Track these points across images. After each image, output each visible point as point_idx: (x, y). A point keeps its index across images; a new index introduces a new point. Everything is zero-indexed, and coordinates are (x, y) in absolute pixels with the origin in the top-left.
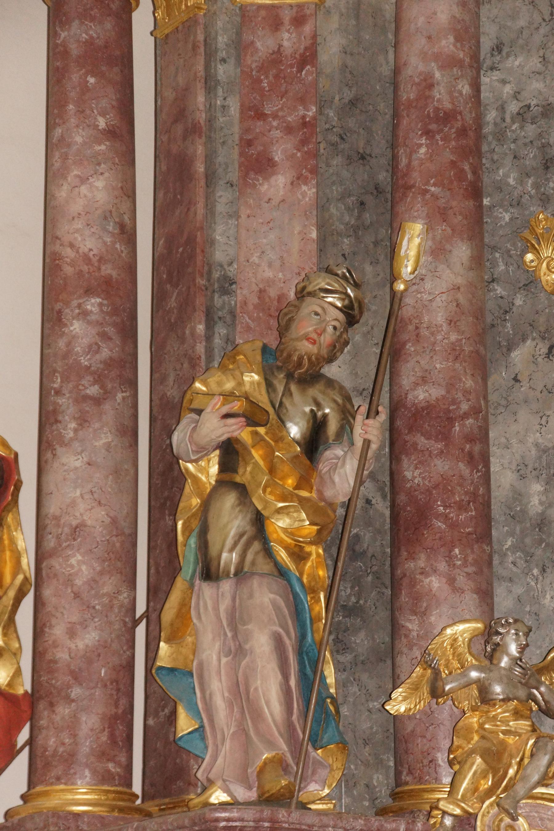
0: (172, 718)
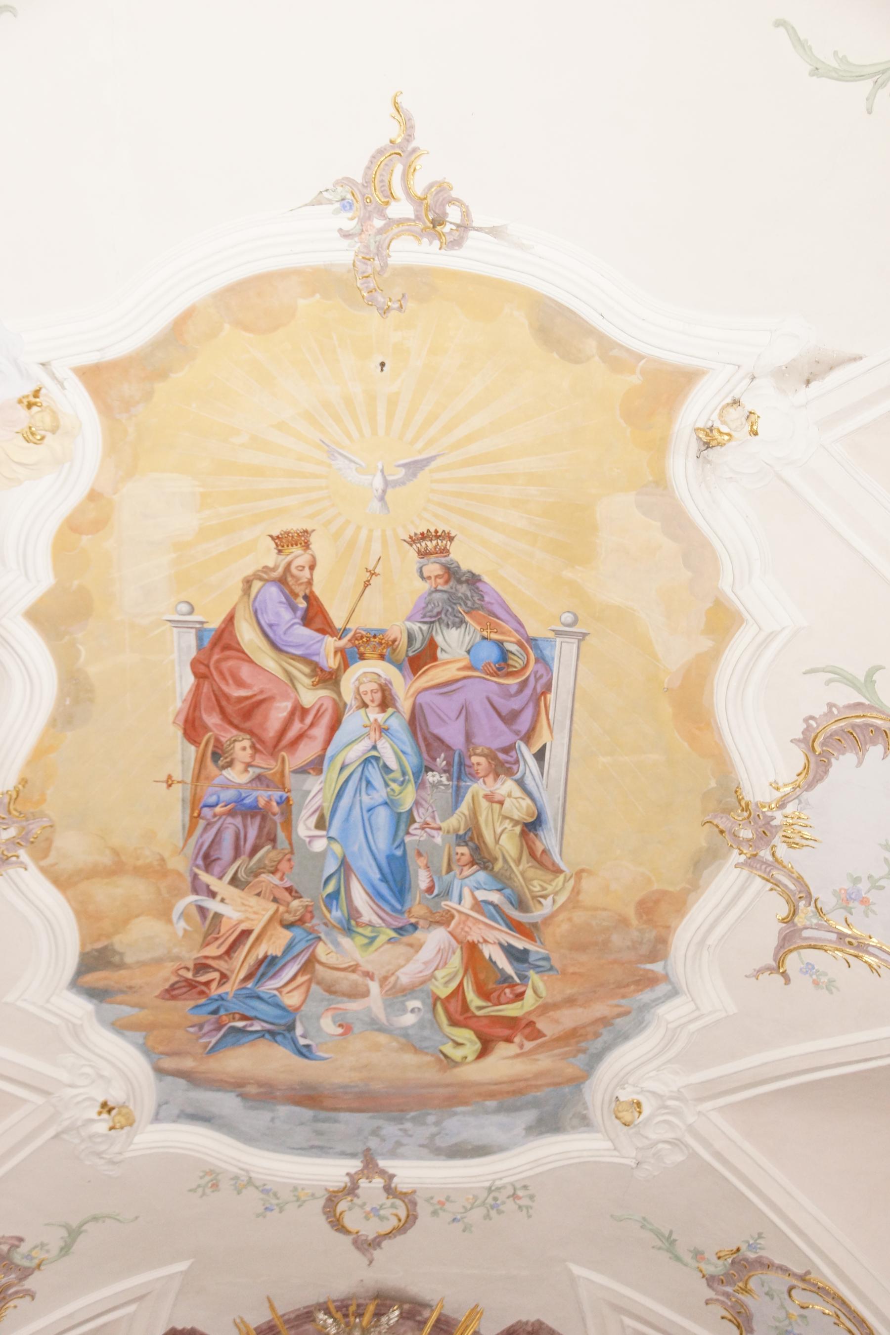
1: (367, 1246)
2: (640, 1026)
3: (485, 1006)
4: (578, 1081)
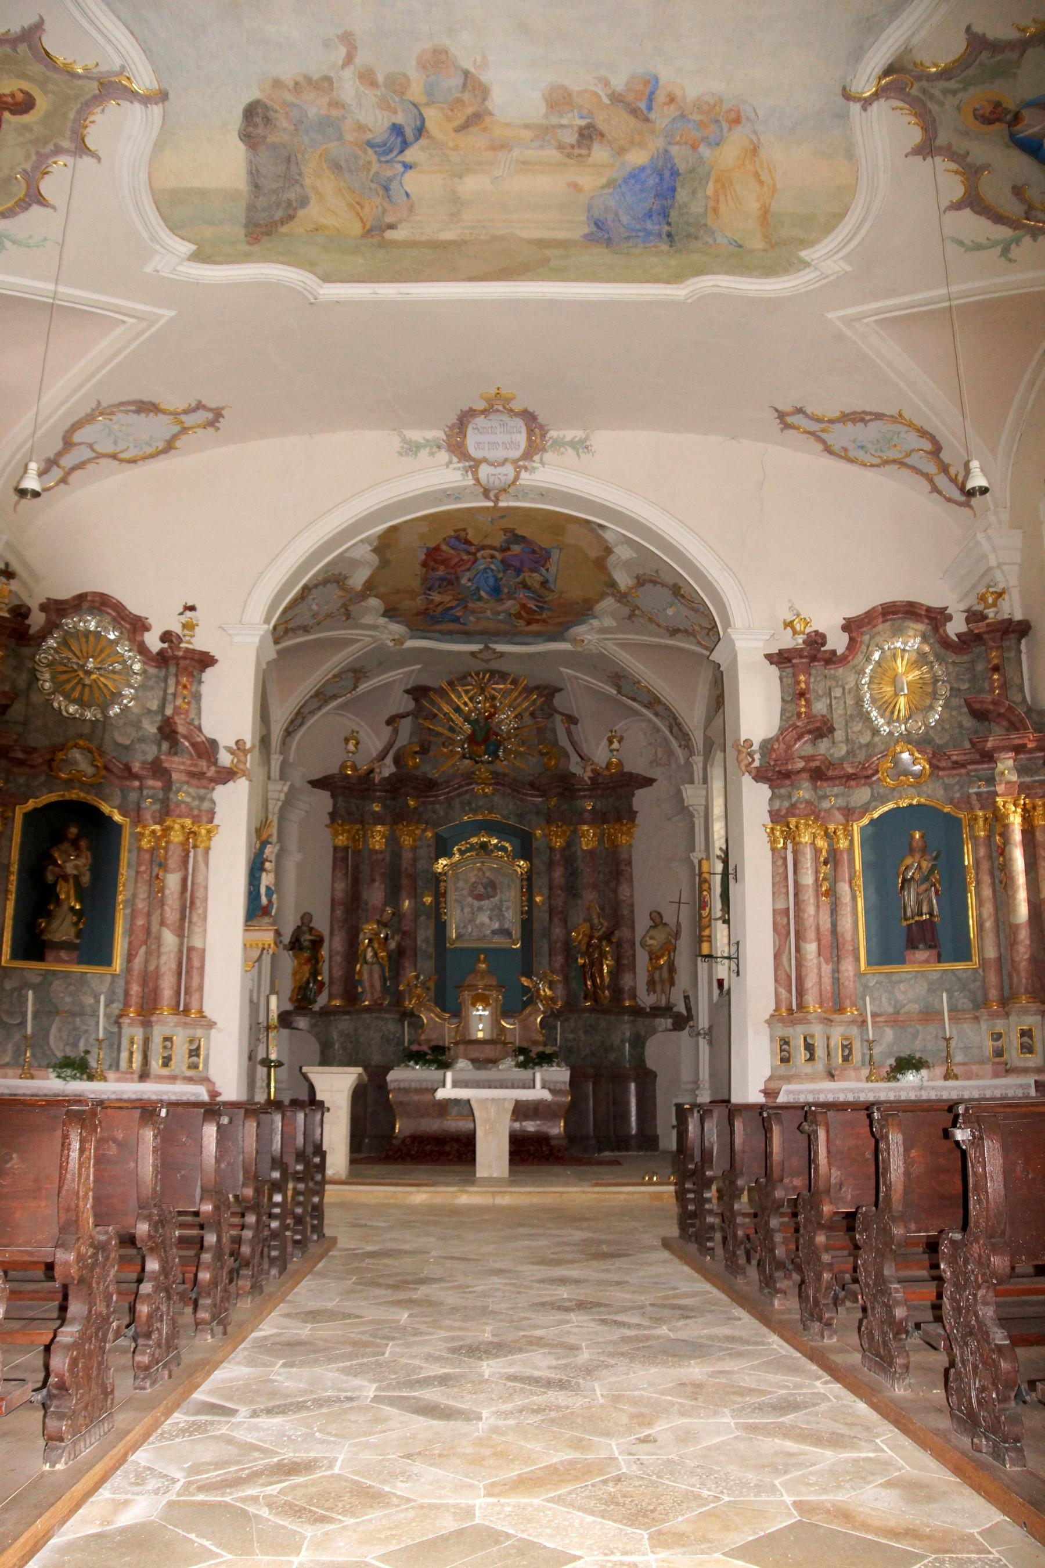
0: (356, 988)
1: (487, 661)
2: (583, 622)
3: (528, 615)
4: (562, 633)
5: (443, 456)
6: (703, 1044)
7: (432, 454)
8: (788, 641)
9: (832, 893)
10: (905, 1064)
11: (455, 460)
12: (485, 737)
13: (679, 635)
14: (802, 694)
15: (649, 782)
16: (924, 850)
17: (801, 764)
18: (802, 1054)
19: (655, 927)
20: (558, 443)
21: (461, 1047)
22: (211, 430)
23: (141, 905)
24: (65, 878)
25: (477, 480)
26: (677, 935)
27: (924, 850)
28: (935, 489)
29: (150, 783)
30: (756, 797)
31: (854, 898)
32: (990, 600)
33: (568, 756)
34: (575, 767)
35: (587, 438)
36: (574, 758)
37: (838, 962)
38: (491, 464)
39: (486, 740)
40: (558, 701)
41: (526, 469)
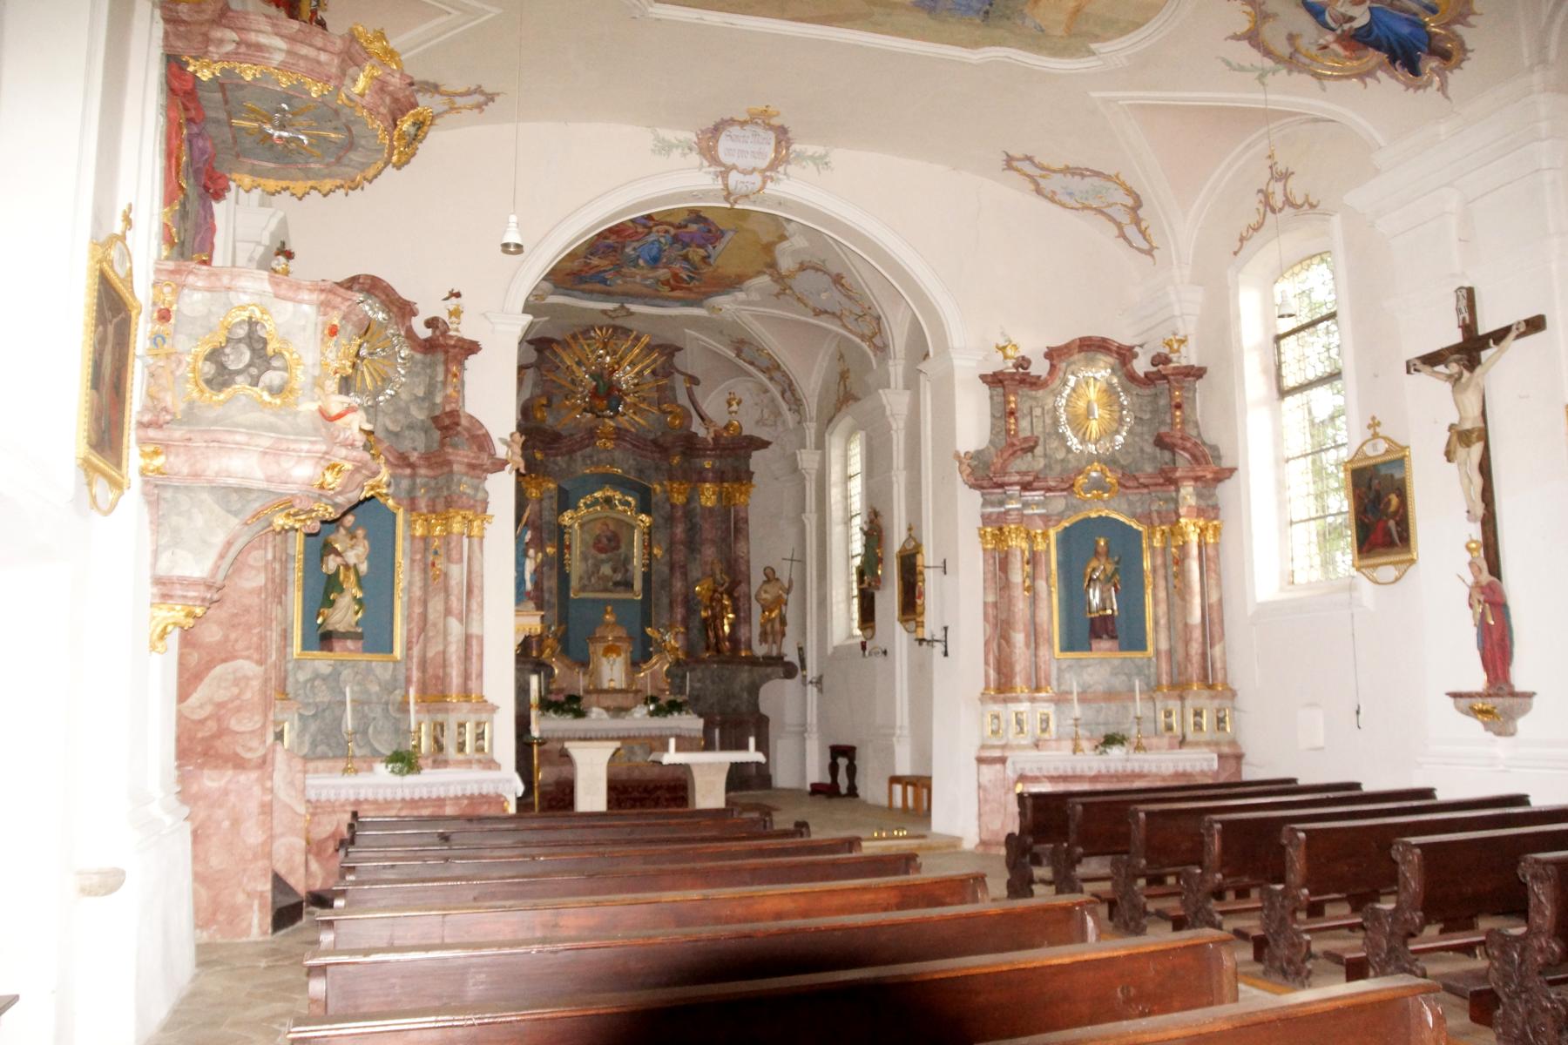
5: (695, 158)
6: (812, 691)
7: (684, 155)
8: (998, 364)
9: (1031, 589)
10: (1110, 740)
11: (706, 163)
12: (606, 393)
13: (824, 317)
14: (1012, 413)
15: (765, 444)
16: (1108, 554)
17: (1016, 478)
18: (1014, 728)
19: (768, 581)
20: (800, 156)
21: (594, 697)
22: (476, 111)
23: (417, 592)
24: (347, 567)
25: (726, 186)
26: (788, 591)
27: (1108, 554)
28: (1123, 236)
29: (423, 471)
30: (969, 503)
31: (1050, 593)
32: (1175, 346)
33: (691, 416)
34: (697, 427)
35: (826, 155)
36: (696, 419)
37: (1036, 648)
38: (744, 172)
39: (608, 394)
40: (678, 360)
41: (772, 179)
